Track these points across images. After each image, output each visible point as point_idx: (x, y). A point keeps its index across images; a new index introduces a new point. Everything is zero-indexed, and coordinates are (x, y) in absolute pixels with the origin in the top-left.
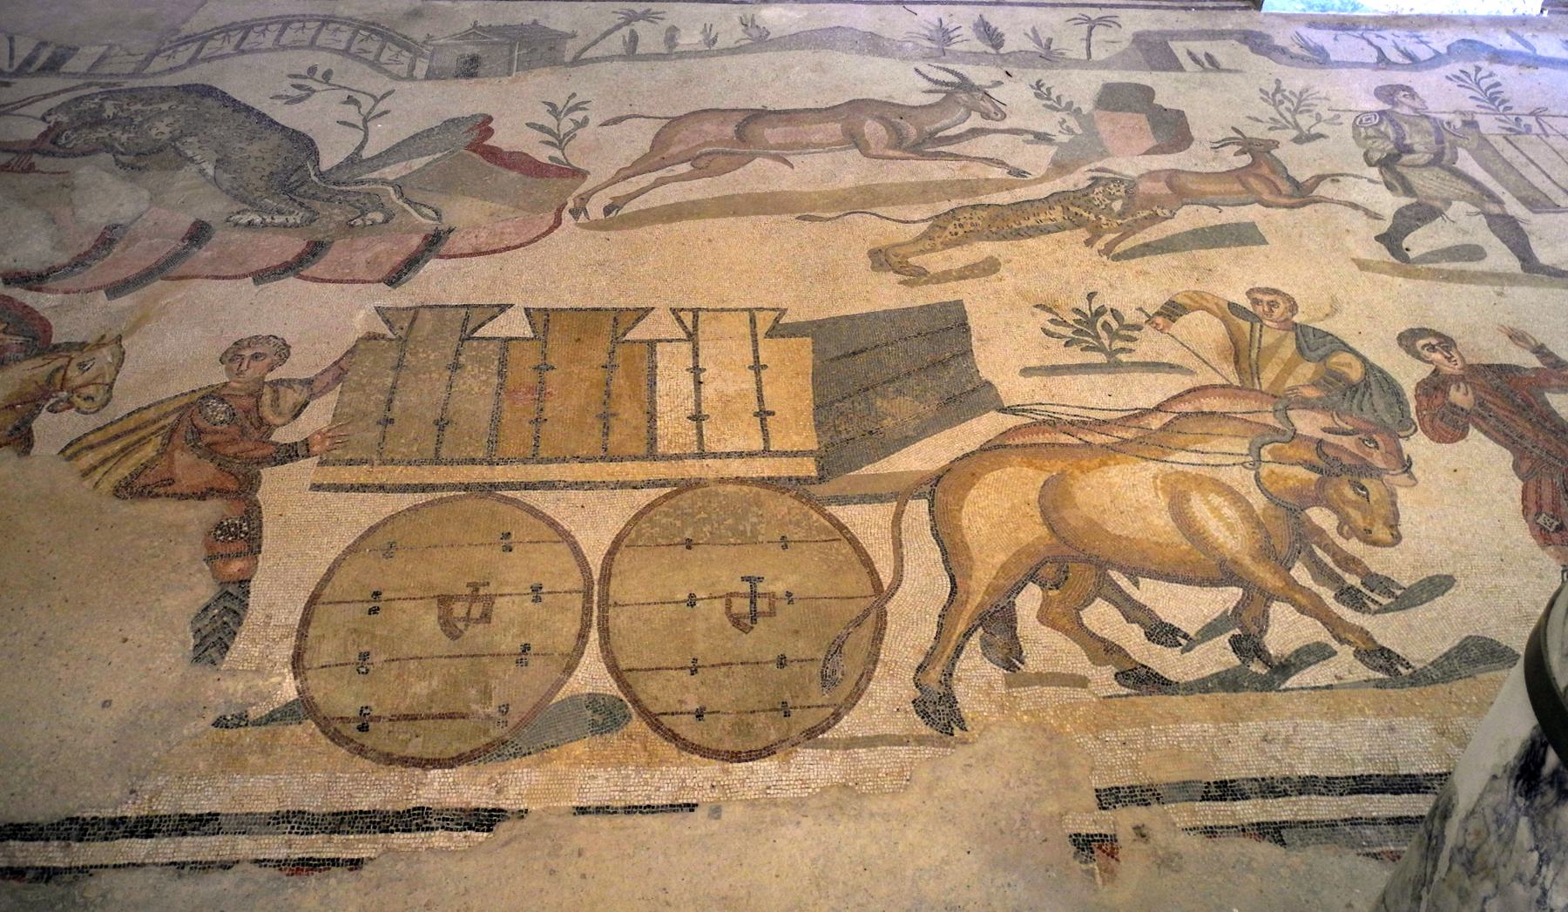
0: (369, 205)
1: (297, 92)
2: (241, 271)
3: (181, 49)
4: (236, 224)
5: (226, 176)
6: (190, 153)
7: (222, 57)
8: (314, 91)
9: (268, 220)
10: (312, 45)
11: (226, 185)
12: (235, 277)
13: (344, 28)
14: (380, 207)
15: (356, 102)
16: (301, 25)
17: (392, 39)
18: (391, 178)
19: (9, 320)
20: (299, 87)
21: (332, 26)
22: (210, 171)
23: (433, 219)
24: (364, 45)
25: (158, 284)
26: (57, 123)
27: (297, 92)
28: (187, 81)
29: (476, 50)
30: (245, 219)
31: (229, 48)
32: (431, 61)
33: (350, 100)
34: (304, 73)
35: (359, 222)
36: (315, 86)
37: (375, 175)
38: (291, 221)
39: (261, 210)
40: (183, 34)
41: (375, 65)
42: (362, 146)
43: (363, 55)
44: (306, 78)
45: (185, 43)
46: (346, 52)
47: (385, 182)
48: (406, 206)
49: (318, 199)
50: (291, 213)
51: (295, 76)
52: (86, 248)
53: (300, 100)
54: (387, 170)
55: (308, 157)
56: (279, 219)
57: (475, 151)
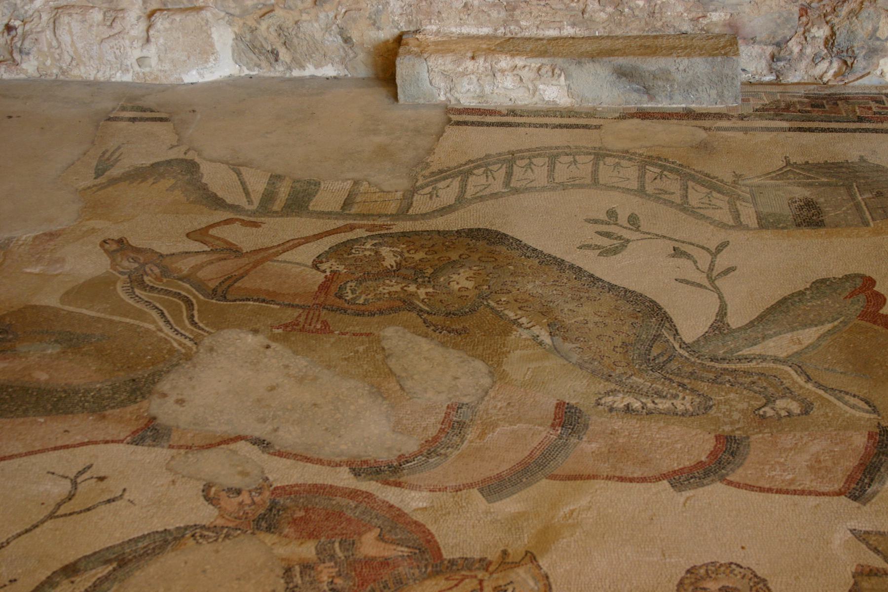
0: (771, 390)
1: (606, 242)
2: (647, 472)
3: (441, 185)
4: (611, 409)
5: (568, 346)
6: (511, 315)
7: (494, 196)
8: (628, 241)
9: (650, 405)
10: (595, 182)
11: (575, 358)
12: (643, 480)
13: (624, 163)
14: (788, 393)
15: (689, 256)
16: (571, 159)
17: (693, 178)
18: (782, 355)
19: (380, 523)
20: (608, 235)
21: (609, 160)
22: (548, 340)
23: (867, 412)
24: (659, 184)
25: (544, 486)
26: (334, 273)
27: (606, 242)
28: (471, 224)
29: (806, 193)
30: (620, 401)
31: (497, 186)
32: (755, 205)
33: (677, 253)
34: (603, 216)
35: (768, 411)
36: (626, 234)
37: (757, 350)
38: (680, 408)
39: (634, 391)
40: (434, 168)
41: (684, 207)
42: (722, 312)
43: (666, 197)
44: (608, 224)
45: (445, 178)
46: (641, 191)
47: (776, 360)
48: (821, 392)
49: (702, 379)
50: (675, 396)
51: (596, 222)
52: (432, 432)
53: (615, 251)
54: (770, 343)
55: (661, 325)
56: (664, 405)
57: (875, 322)
